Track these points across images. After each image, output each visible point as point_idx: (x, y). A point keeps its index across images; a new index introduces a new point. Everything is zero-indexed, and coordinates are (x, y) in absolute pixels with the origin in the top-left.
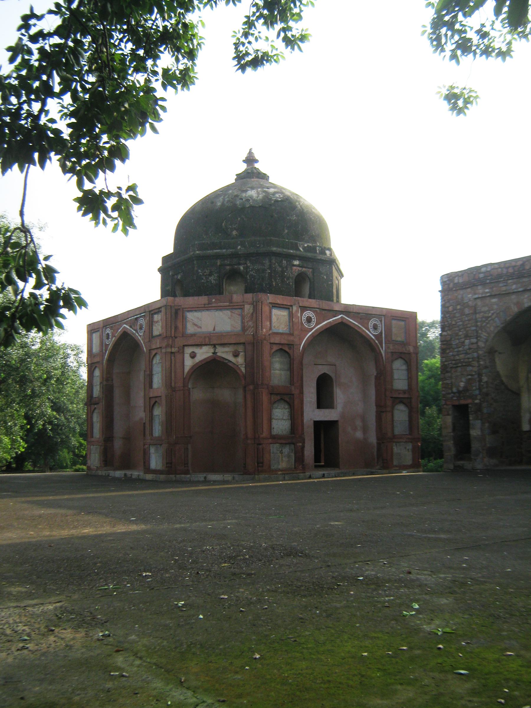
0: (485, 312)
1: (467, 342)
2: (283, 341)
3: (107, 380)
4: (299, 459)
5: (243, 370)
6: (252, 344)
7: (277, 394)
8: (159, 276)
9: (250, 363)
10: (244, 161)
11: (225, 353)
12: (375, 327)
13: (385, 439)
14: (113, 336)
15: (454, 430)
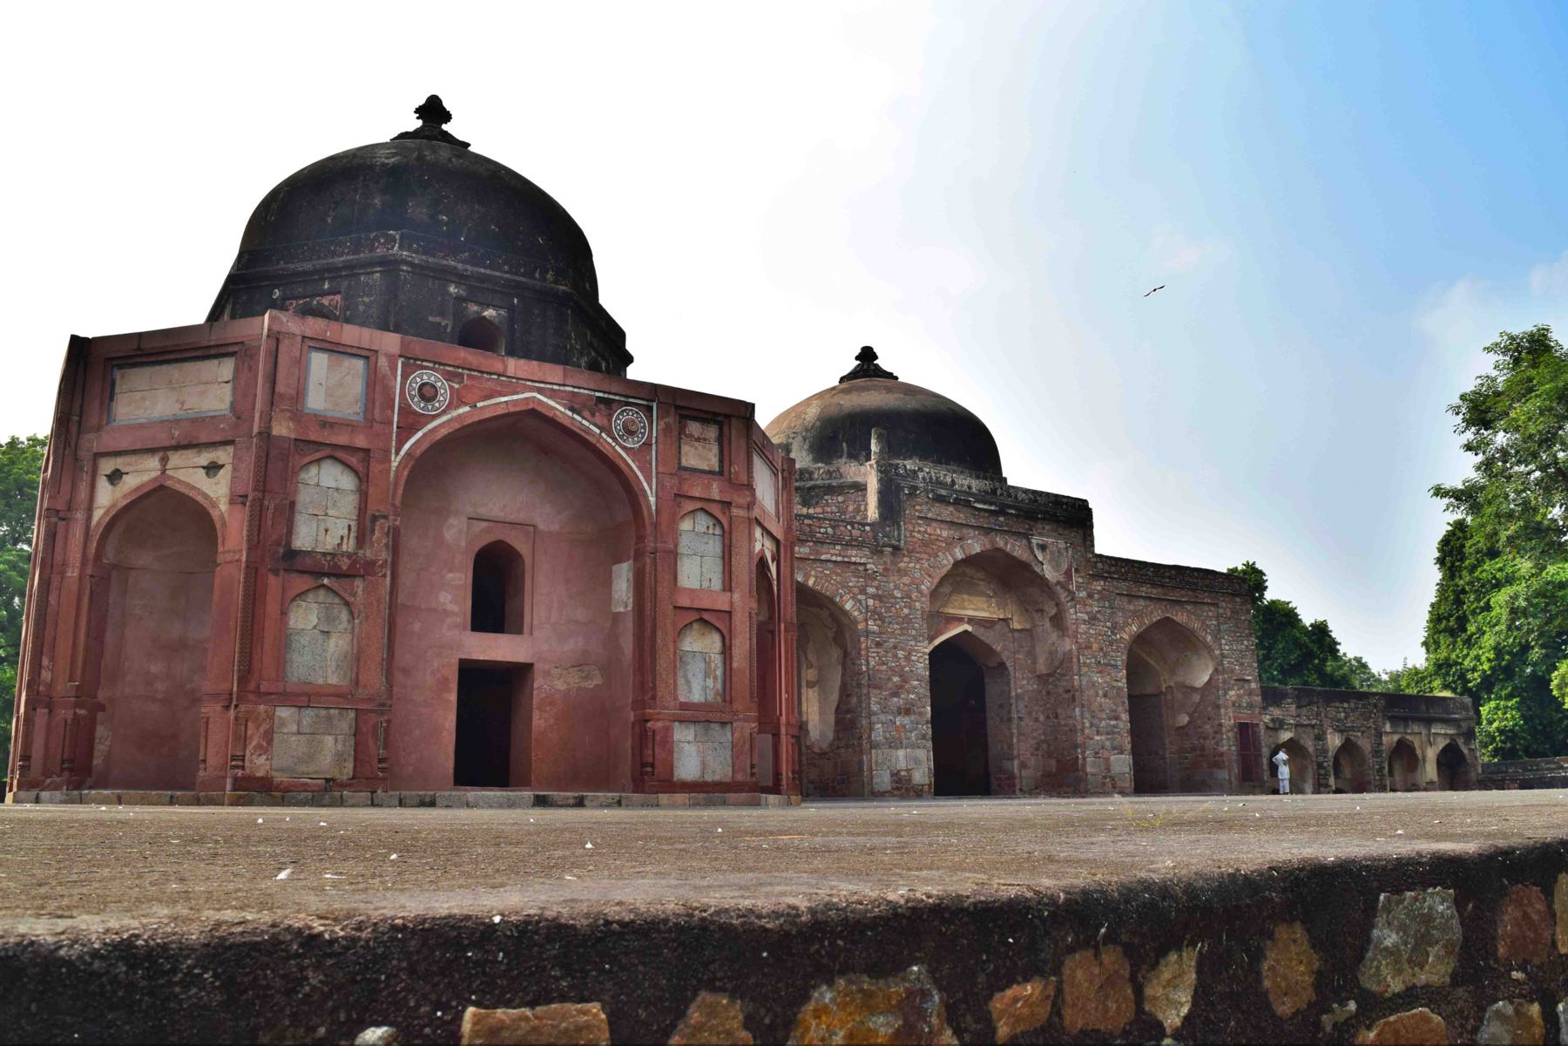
14: (457, 400)
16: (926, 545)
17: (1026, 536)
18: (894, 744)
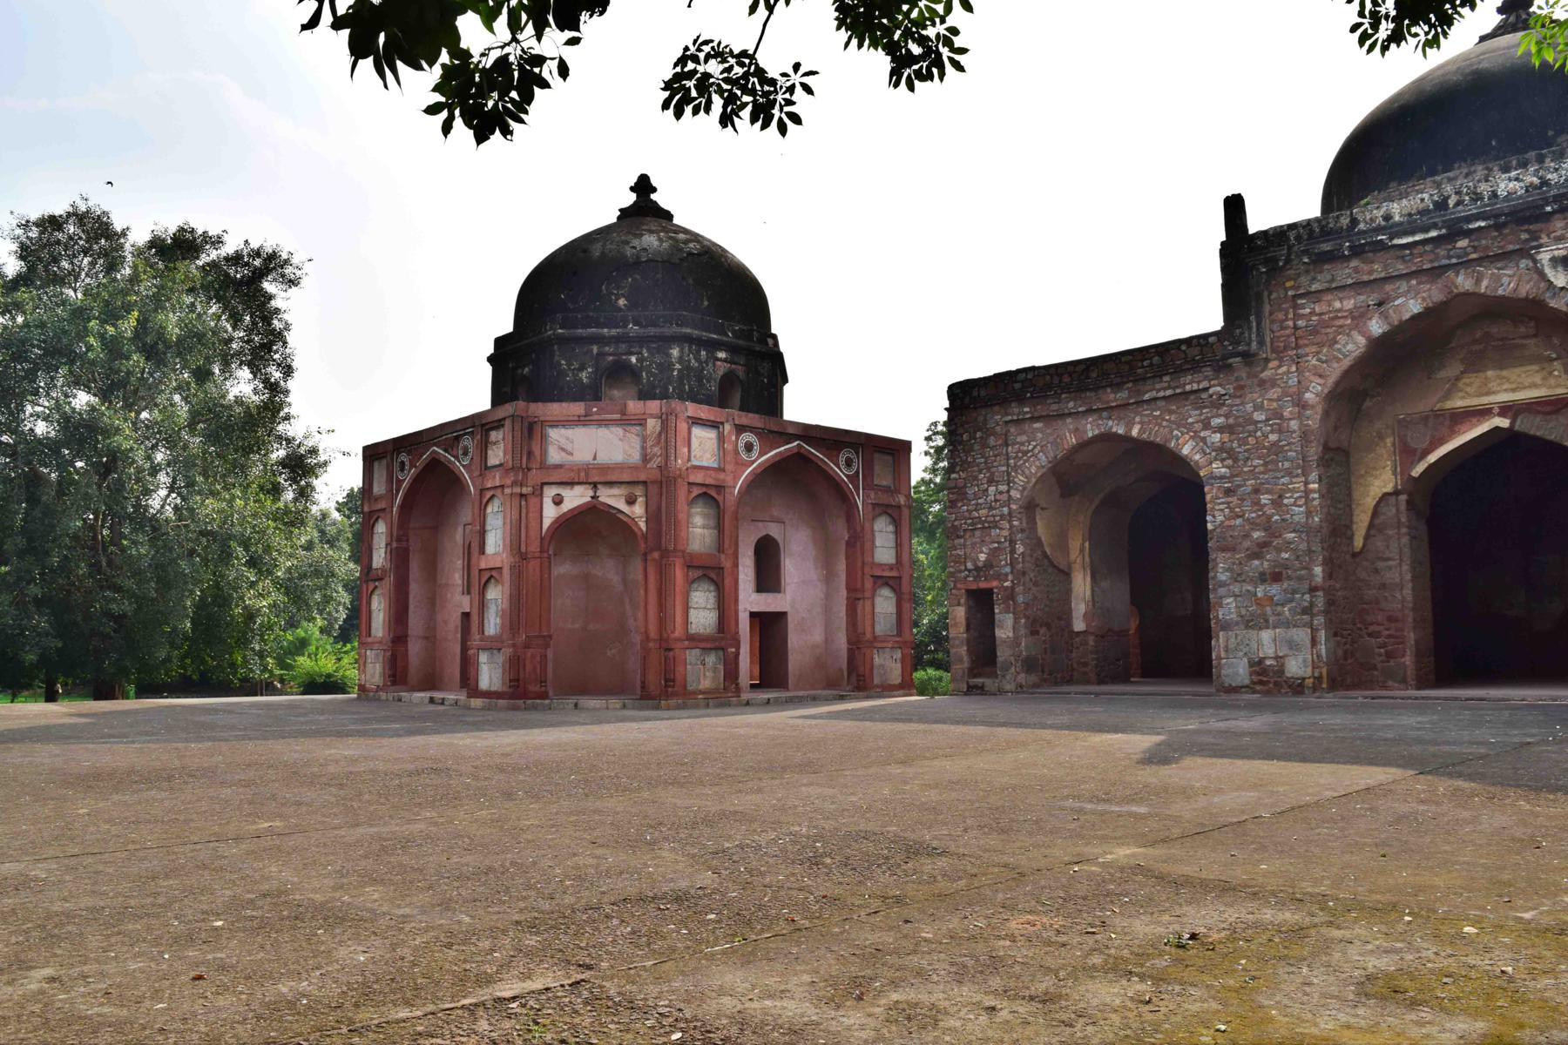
0: (1022, 444)
1: (992, 489)
2: (709, 481)
3: (399, 540)
4: (731, 673)
5: (643, 525)
6: (659, 483)
7: (698, 567)
8: (488, 369)
9: (653, 516)
10: (632, 189)
11: (613, 498)
12: (849, 463)
13: (859, 644)
15: (968, 628)
16: (1315, 332)
17: (1526, 252)
18: (1254, 622)
